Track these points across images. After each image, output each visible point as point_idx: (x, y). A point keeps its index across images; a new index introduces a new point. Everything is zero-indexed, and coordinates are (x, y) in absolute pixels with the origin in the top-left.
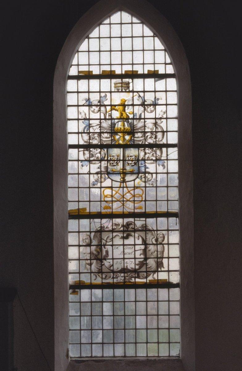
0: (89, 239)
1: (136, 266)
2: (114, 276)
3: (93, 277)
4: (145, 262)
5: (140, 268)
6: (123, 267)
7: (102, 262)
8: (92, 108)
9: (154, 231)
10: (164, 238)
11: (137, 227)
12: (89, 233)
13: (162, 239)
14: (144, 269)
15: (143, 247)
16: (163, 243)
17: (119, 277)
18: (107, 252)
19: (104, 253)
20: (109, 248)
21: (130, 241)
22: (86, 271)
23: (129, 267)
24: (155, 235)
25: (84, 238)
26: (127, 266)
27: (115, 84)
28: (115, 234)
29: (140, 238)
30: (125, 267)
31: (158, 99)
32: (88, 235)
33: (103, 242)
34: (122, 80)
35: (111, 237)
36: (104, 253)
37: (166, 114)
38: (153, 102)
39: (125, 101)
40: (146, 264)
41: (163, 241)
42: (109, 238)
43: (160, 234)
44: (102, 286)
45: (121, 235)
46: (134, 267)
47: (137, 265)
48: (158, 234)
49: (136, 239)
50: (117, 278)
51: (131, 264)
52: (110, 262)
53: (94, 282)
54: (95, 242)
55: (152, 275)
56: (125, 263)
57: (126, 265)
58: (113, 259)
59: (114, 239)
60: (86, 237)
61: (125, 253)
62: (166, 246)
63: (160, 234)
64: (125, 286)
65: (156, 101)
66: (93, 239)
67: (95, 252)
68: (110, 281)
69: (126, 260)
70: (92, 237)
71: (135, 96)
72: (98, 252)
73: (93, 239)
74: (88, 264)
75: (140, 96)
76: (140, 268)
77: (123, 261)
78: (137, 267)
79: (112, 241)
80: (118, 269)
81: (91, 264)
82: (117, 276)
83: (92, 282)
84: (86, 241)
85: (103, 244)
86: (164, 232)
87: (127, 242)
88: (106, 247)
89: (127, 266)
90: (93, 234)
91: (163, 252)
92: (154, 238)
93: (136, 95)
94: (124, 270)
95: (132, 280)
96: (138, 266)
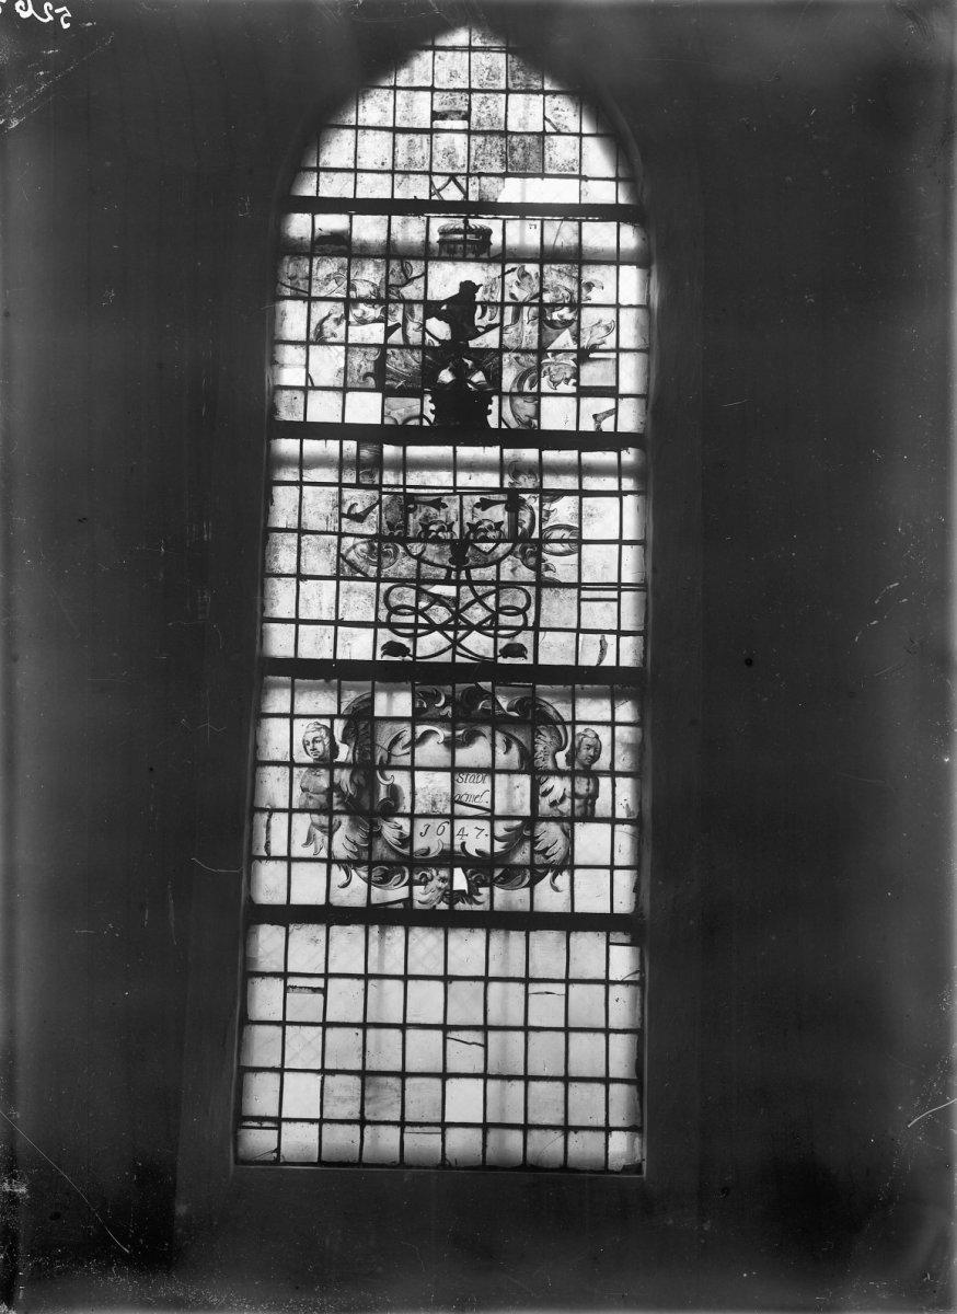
0: (326, 741)
1: (496, 842)
2: (417, 877)
3: (339, 875)
4: (527, 833)
5: (511, 849)
6: (447, 847)
7: (373, 824)
8: (356, 308)
9: (564, 723)
10: (598, 750)
11: (501, 708)
12: (326, 722)
13: (591, 752)
14: (521, 856)
15: (524, 781)
16: (595, 766)
17: (432, 878)
18: (394, 791)
19: (383, 795)
20: (401, 779)
21: (476, 753)
22: (309, 852)
23: (471, 850)
24: (566, 738)
25: (310, 737)
26: (463, 844)
27: (443, 232)
28: (420, 729)
29: (515, 748)
30: (457, 848)
31: (590, 286)
32: (325, 727)
33: (380, 754)
34: (466, 222)
35: (407, 738)
36: (383, 795)
37: (614, 334)
38: (571, 293)
39: (475, 288)
40: (534, 840)
41: (595, 758)
42: (400, 744)
43: (585, 736)
44: (373, 916)
45: (443, 733)
46: (488, 850)
47: (500, 840)
48: (580, 734)
49: (500, 751)
50: (425, 884)
51: (476, 839)
52: (400, 828)
53: (341, 898)
54: (345, 753)
55: (550, 875)
56: (456, 832)
57: (458, 841)
58: (412, 817)
59: (418, 750)
60: (317, 734)
61: (454, 790)
62: (605, 782)
63: (585, 736)
64: (446, 920)
65: (584, 291)
66: (344, 741)
67: (347, 787)
68: (395, 893)
69: (459, 824)
70: (338, 734)
71: (509, 272)
72: (358, 787)
73: (344, 741)
74: (321, 828)
75: (524, 275)
76: (511, 849)
77: (448, 827)
78: (499, 847)
79: (413, 753)
80: (428, 850)
81: (330, 831)
82: (424, 875)
83: (331, 900)
84: (314, 749)
85: (378, 762)
86: (598, 729)
87: (465, 756)
88: (388, 774)
89: (463, 844)
90: (339, 726)
91: (594, 795)
92: (562, 749)
93: (513, 270)
94: (451, 858)
95: (480, 894)
96: (503, 844)
